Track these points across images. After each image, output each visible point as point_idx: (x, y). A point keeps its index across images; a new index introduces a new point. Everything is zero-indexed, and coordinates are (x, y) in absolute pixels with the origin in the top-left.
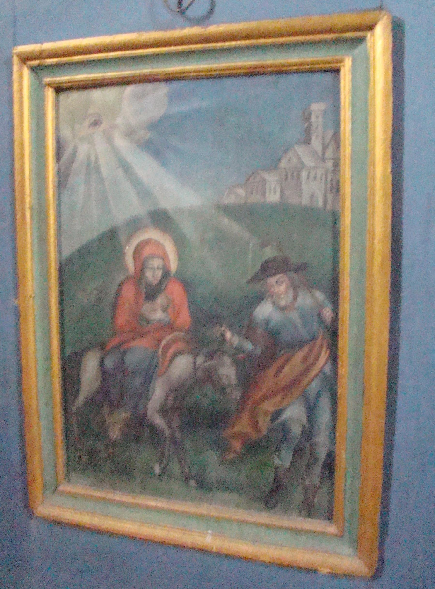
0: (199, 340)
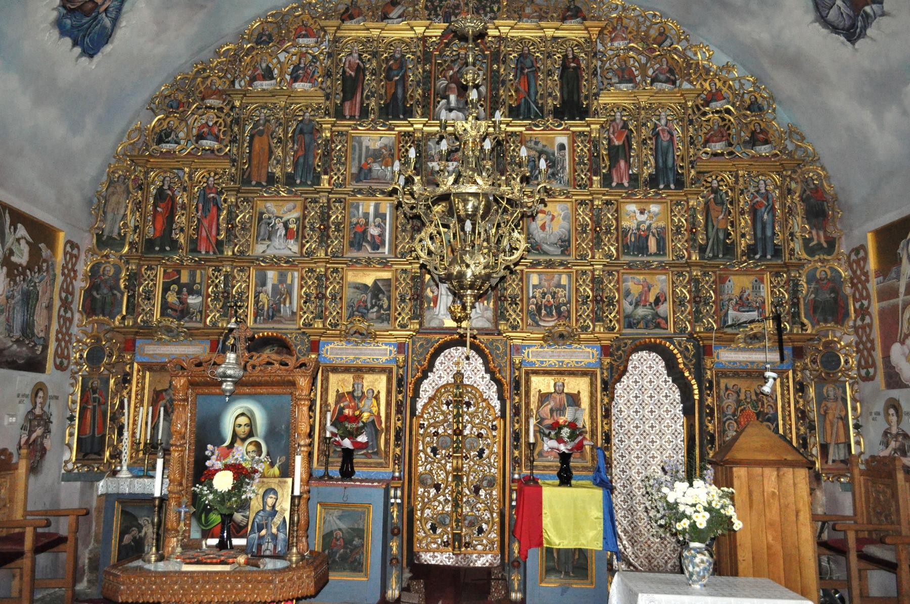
0: (345, 547)
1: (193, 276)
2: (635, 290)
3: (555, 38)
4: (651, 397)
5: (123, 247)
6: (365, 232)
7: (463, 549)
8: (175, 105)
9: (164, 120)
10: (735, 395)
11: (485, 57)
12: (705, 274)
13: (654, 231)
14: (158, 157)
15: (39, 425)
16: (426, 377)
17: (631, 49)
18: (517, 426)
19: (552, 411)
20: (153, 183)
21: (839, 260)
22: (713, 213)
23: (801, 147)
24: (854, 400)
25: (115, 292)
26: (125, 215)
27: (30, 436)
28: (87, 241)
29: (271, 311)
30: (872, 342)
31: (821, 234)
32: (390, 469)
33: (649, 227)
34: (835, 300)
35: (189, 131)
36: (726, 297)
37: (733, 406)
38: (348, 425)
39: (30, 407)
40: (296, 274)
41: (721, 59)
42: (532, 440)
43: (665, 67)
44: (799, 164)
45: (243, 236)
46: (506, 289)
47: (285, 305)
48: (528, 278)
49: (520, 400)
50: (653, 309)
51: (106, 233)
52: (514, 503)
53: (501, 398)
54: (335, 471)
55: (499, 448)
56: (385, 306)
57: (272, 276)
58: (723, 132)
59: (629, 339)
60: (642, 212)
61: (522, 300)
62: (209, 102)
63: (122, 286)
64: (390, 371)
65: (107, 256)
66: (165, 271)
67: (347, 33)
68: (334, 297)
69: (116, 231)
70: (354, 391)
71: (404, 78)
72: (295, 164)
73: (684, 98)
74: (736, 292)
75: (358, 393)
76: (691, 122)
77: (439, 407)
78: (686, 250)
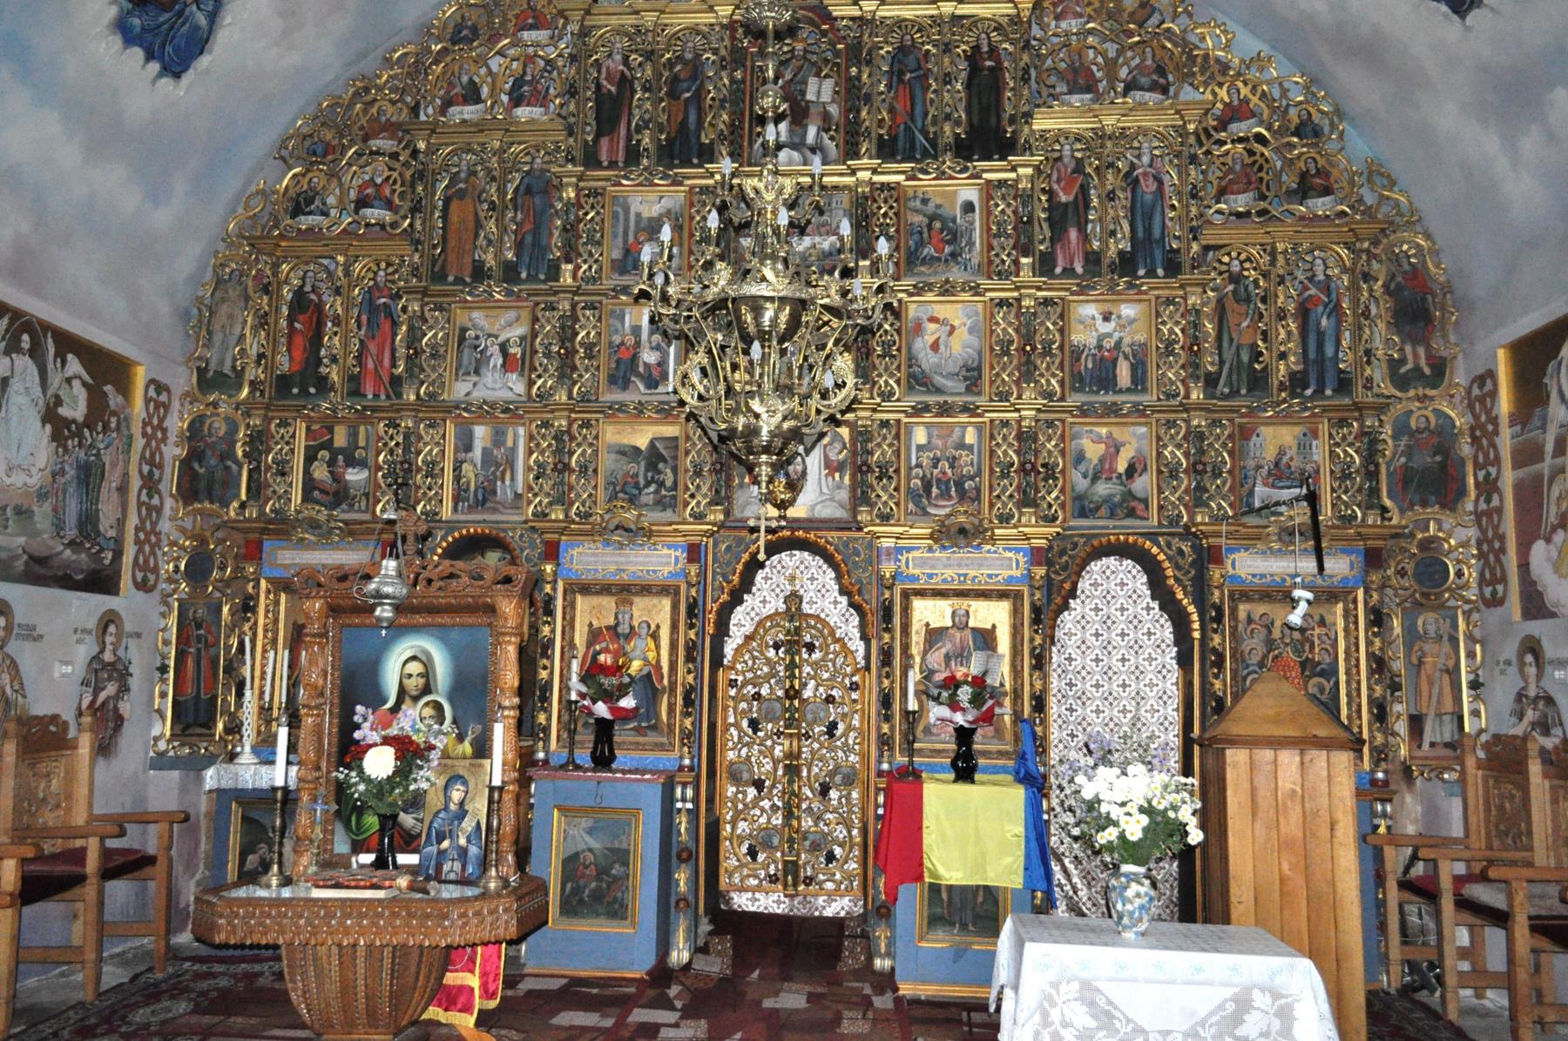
0: (598, 878)
1: (354, 435)
2: (1094, 451)
3: (956, 19)
4: (1123, 635)
5: (240, 388)
6: (635, 358)
7: (802, 887)
8: (319, 150)
9: (304, 175)
10: (1264, 631)
11: (837, 54)
12: (1215, 423)
13: (1127, 350)
14: (291, 239)
15: (110, 679)
16: (741, 602)
17: (1091, 32)
18: (886, 683)
19: (947, 658)
20: (286, 281)
21: (1452, 396)
22: (1231, 318)
23: (1388, 198)
24: (1471, 638)
25: (229, 463)
26: (242, 337)
27: (95, 695)
28: (182, 380)
29: (480, 492)
30: (1502, 538)
31: (1421, 351)
32: (677, 752)
33: (1118, 344)
34: (1443, 466)
35: (344, 192)
36: (1251, 463)
37: (1261, 650)
38: (606, 681)
39: (97, 650)
40: (521, 431)
41: (1249, 45)
42: (912, 705)
43: (1149, 62)
44: (1383, 230)
45: (434, 368)
46: (871, 453)
47: (503, 481)
48: (909, 433)
49: (892, 638)
50: (1122, 484)
51: (213, 366)
52: (881, 811)
53: (865, 637)
54: (583, 756)
55: (862, 722)
56: (669, 483)
57: (481, 433)
58: (1252, 176)
59: (1082, 536)
60: (1106, 318)
61: (897, 471)
62: (376, 144)
63: (240, 453)
64: (677, 593)
65: (215, 405)
66: (308, 428)
67: (602, 20)
68: (584, 469)
69: (228, 363)
70: (617, 625)
71: (699, 96)
72: (519, 246)
73: (1182, 118)
74: (1270, 454)
75: (624, 629)
76: (1193, 159)
77: (762, 653)
78: (1183, 381)
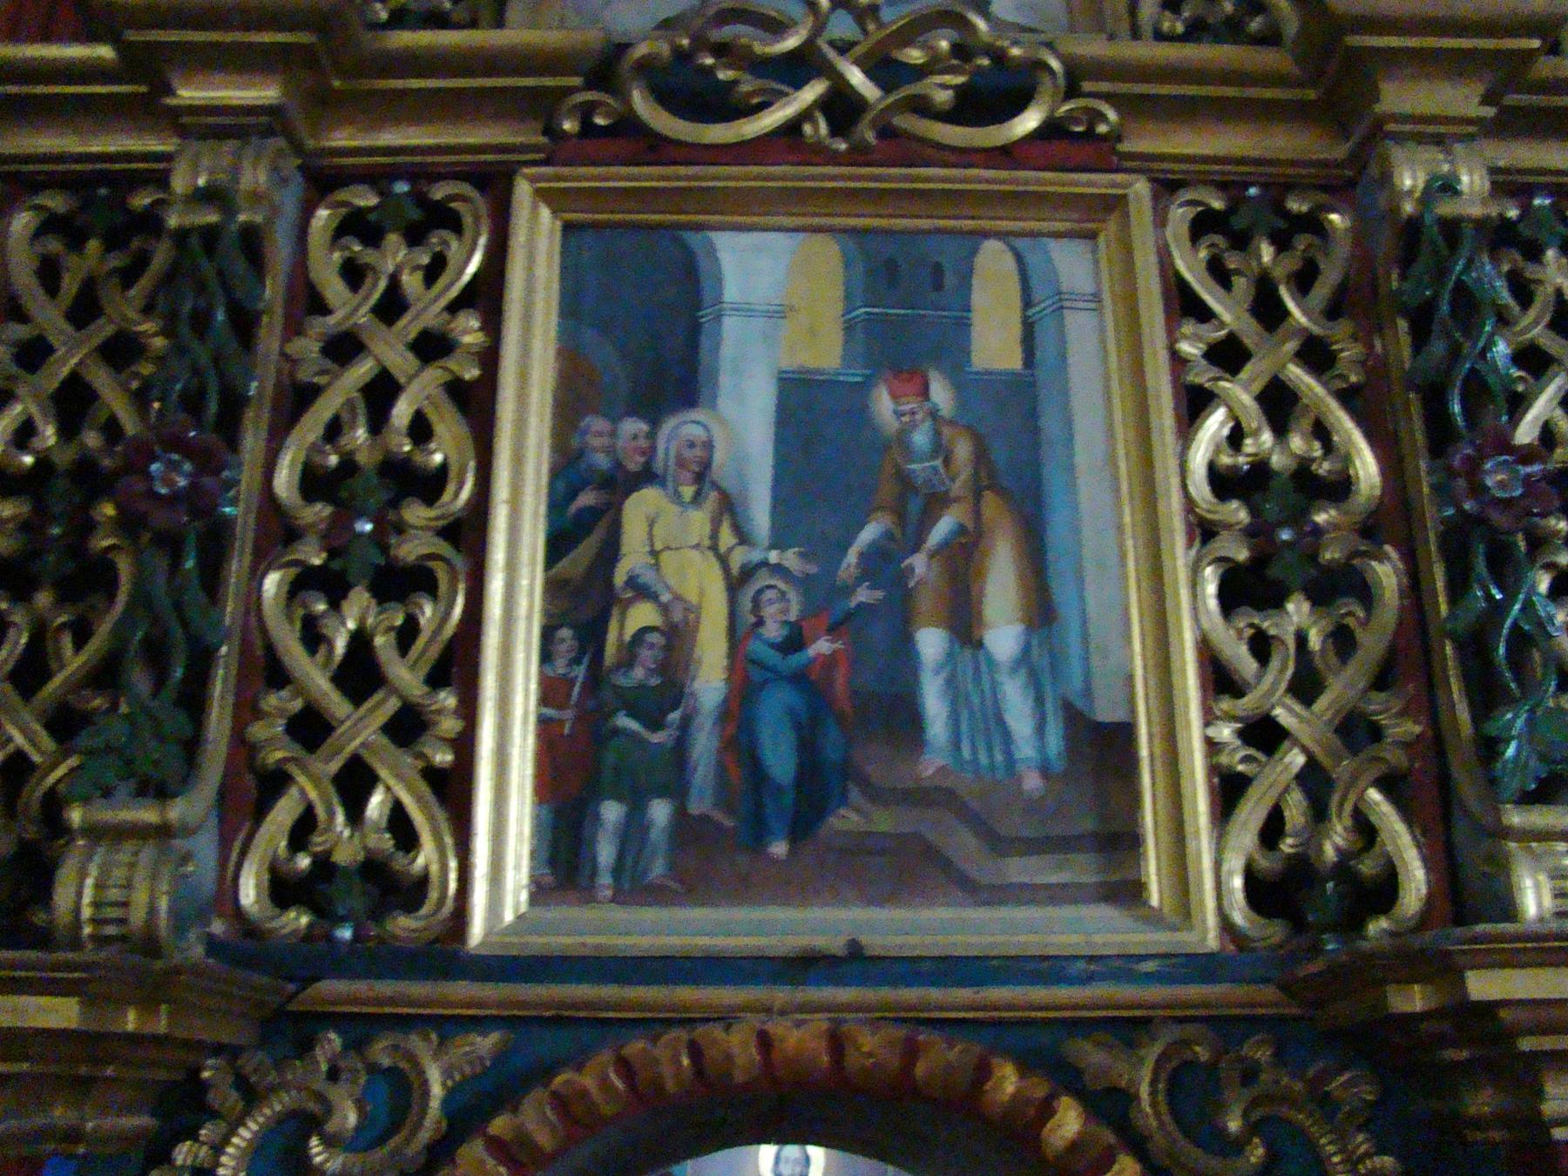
40: (1071, 265)
47: (965, 627)
